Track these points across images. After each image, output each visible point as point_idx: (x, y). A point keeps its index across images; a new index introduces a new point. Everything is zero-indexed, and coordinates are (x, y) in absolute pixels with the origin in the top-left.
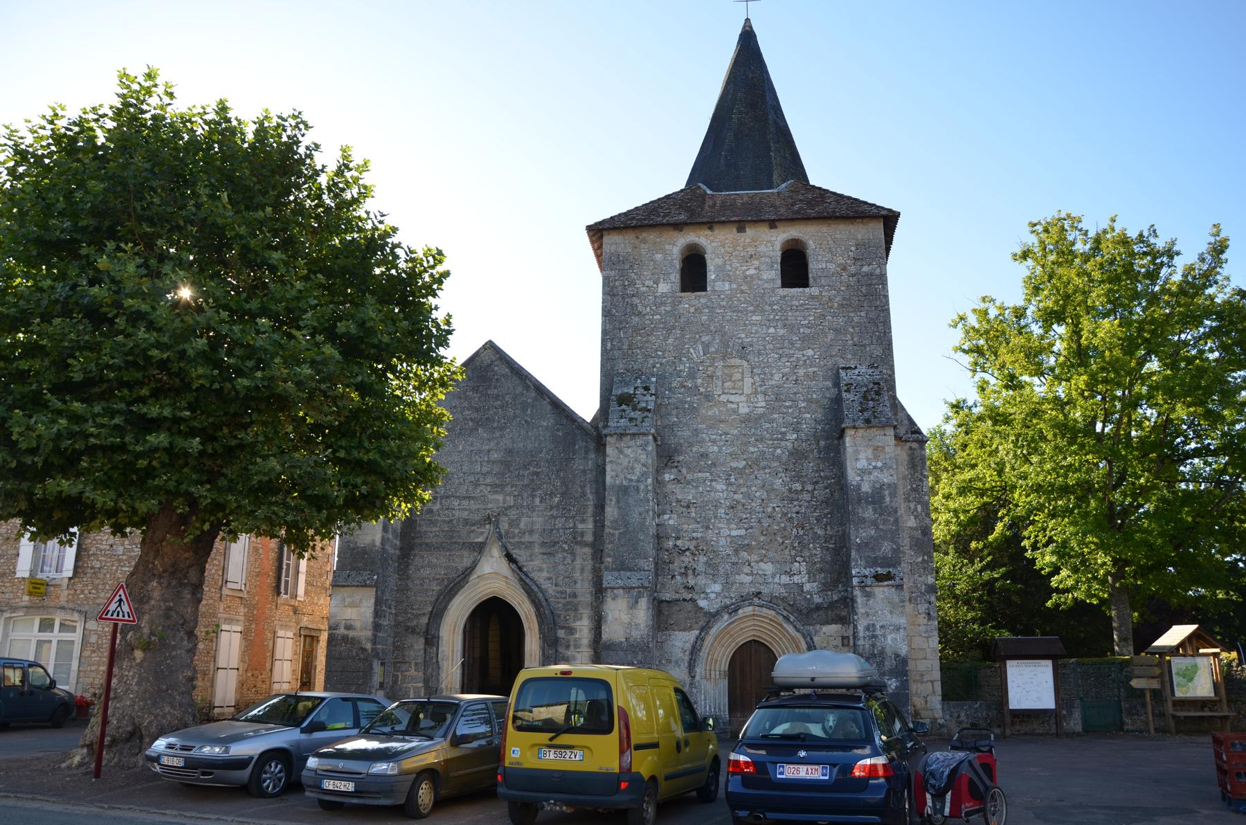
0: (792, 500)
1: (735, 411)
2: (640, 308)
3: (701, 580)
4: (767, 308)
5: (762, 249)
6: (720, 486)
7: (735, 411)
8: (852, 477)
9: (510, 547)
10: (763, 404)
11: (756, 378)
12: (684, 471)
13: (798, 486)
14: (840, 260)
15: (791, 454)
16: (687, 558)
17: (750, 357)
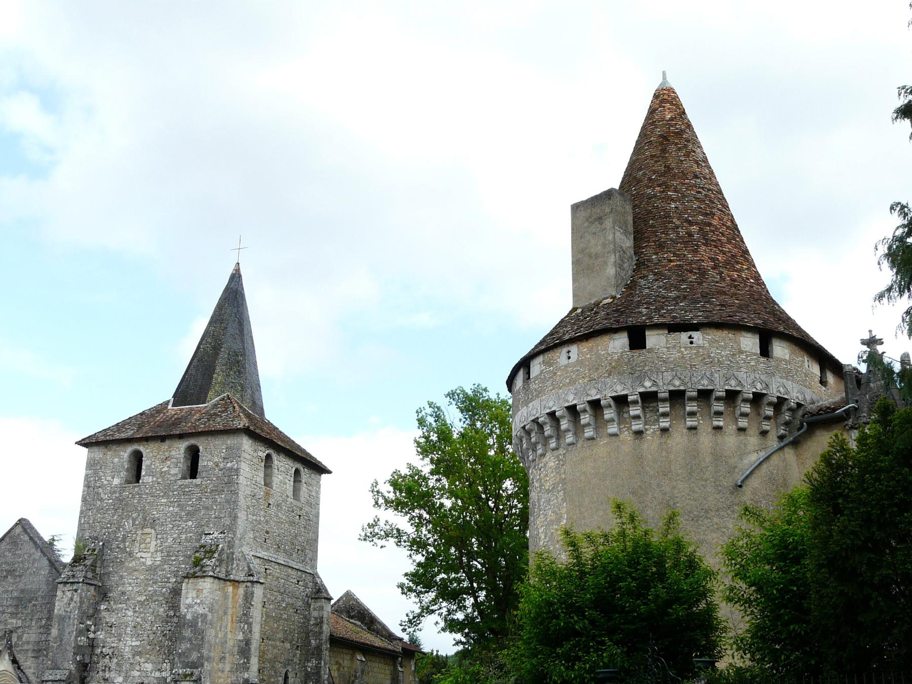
0: (167, 622)
2: (102, 495)
3: (113, 674)
4: (171, 493)
5: (173, 453)
6: (130, 613)
7: (144, 564)
8: (183, 610)
9: (16, 653)
11: (159, 541)
13: (172, 613)
15: (171, 592)
16: (107, 660)
17: (157, 527)
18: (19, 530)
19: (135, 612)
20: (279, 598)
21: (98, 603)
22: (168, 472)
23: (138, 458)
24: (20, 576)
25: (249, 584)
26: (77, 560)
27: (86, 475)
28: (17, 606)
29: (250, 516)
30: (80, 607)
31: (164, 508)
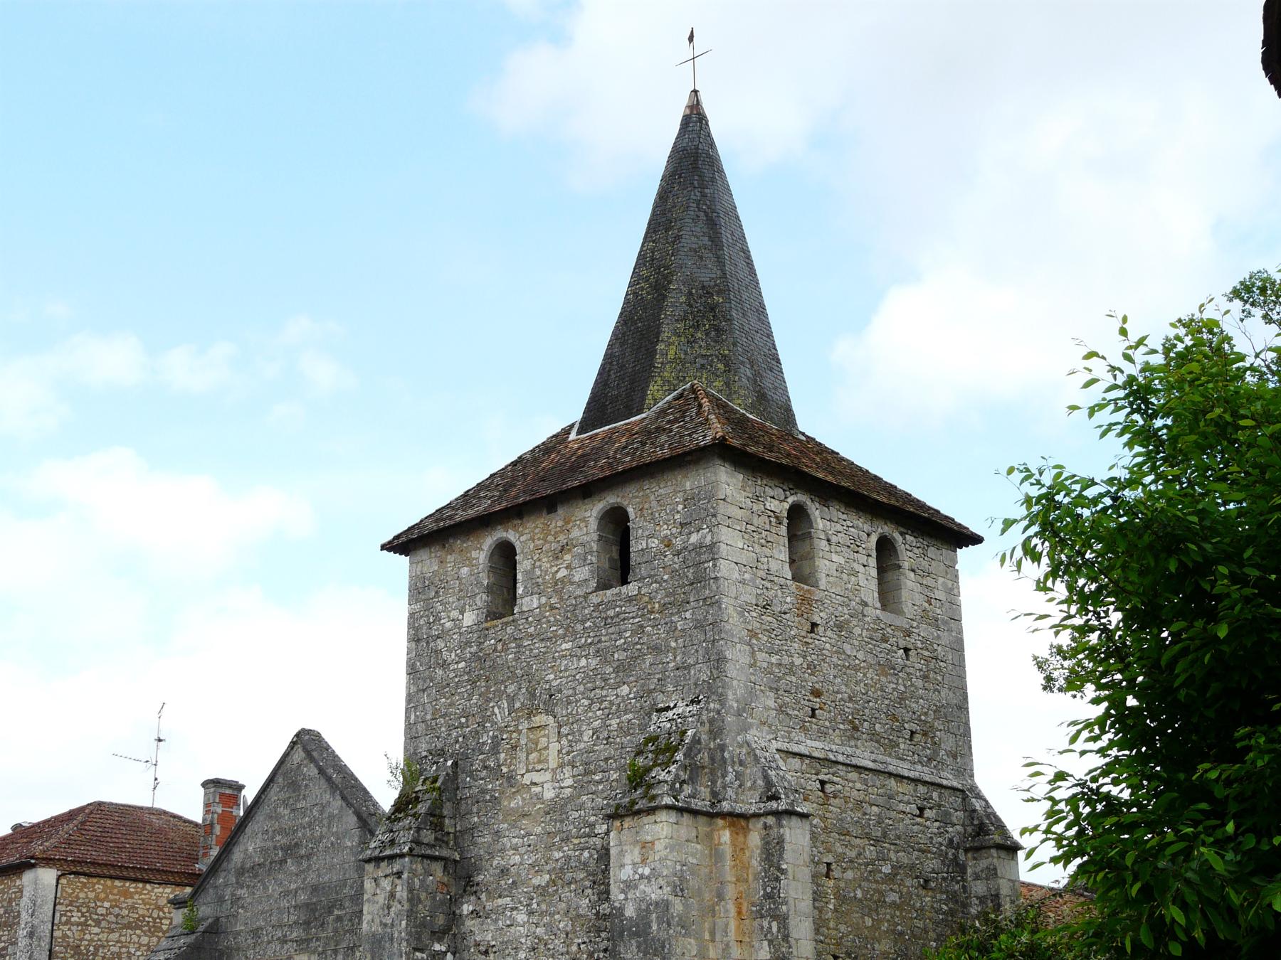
0: (599, 931)
1: (539, 797)
2: (445, 655)
4: (579, 627)
6: (521, 917)
8: (617, 895)
11: (564, 742)
12: (483, 897)
17: (558, 710)
18: (299, 755)
19: (531, 913)
20: (871, 852)
21: (455, 901)
22: (568, 580)
23: (506, 554)
24: (309, 857)
25: (771, 820)
26: (402, 805)
27: (411, 615)
28: (307, 923)
29: (761, 656)
30: (411, 914)
31: (568, 664)
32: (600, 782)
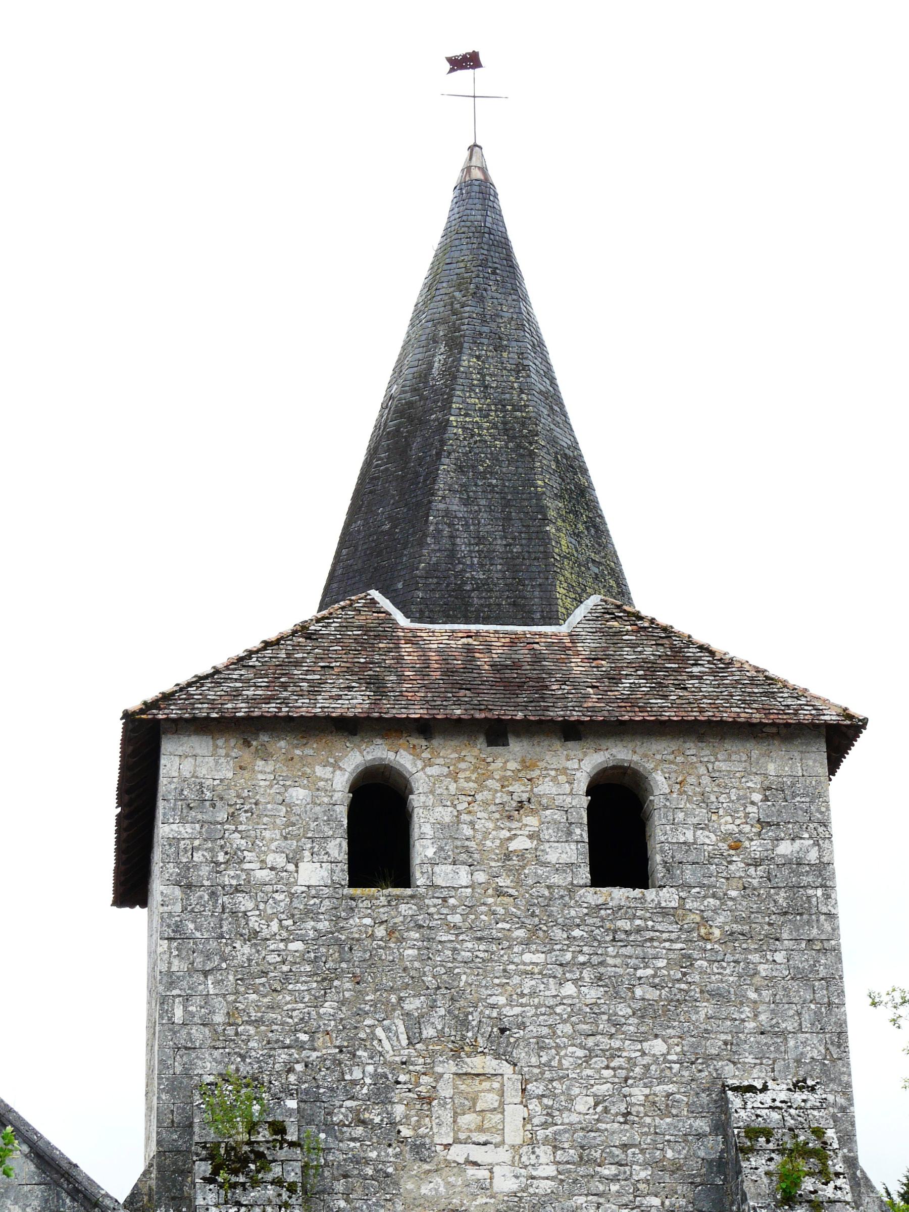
1: (484, 1188)
2: (254, 922)
4: (558, 934)
5: (546, 788)
7: (484, 1188)
10: (551, 1171)
11: (534, 1105)
14: (727, 825)
17: (520, 1054)
31: (531, 985)
32: (615, 1179)
